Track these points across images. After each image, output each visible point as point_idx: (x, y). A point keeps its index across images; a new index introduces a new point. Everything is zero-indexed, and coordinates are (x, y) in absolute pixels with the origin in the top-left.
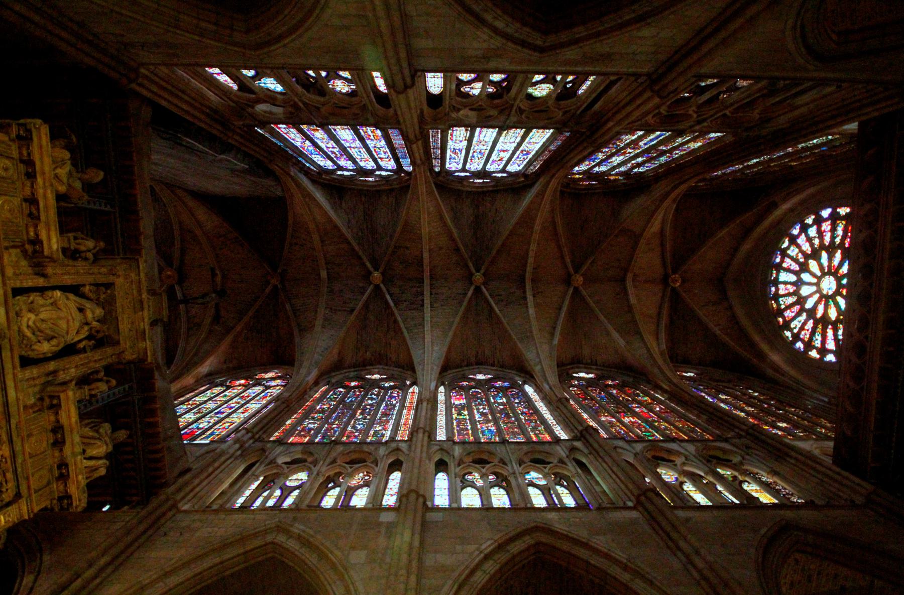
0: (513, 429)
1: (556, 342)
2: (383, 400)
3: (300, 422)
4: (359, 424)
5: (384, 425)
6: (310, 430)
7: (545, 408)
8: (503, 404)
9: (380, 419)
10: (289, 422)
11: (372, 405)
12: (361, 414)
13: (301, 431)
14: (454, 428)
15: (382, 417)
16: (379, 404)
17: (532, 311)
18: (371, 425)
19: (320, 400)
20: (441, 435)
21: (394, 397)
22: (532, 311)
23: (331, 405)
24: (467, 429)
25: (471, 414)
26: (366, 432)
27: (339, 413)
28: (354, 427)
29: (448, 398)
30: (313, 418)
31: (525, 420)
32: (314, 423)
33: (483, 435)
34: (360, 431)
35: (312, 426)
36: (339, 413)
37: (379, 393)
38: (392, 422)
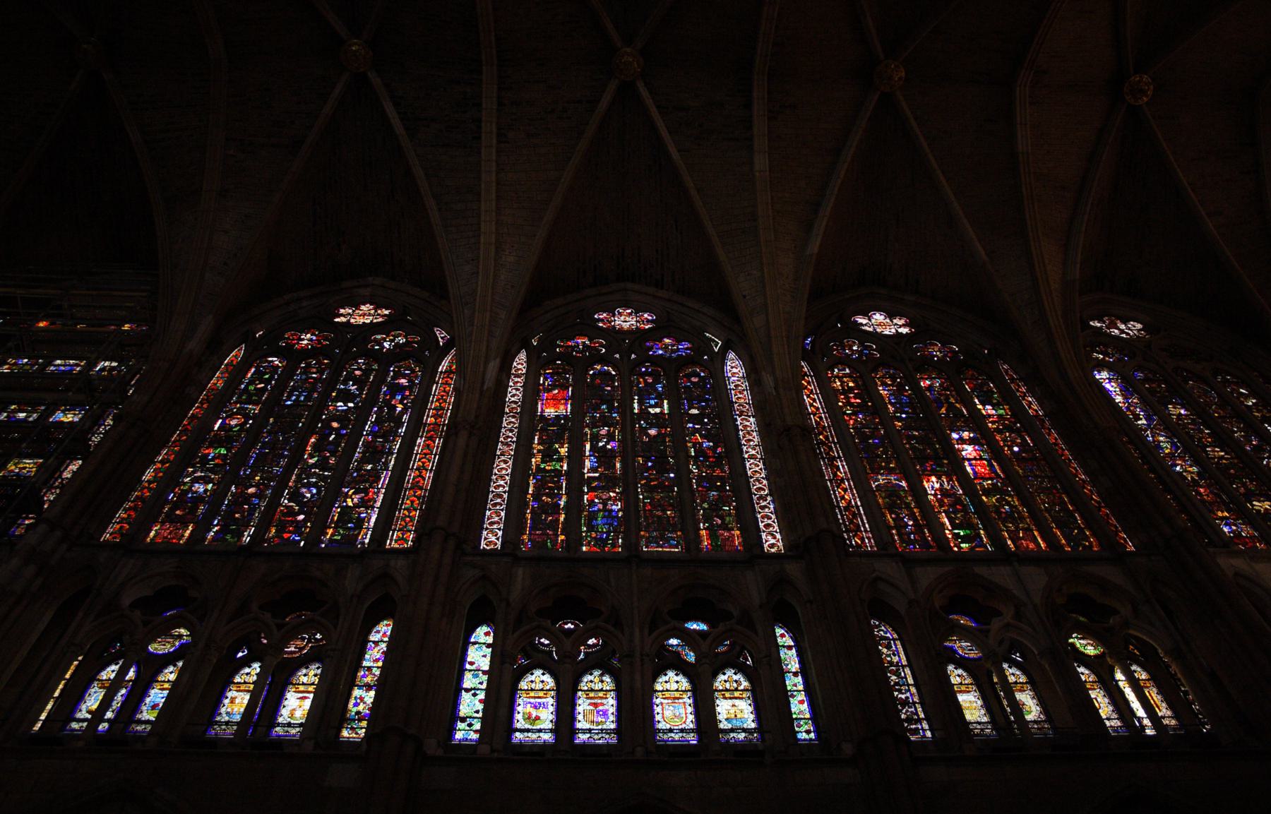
0: (664, 511)
1: (814, 247)
2: (372, 400)
3: (171, 478)
4: (309, 486)
5: (366, 491)
6: (199, 499)
7: (756, 440)
8: (658, 420)
9: (358, 469)
10: (148, 475)
11: (343, 417)
12: (317, 448)
13: (175, 506)
14: (526, 505)
15: (363, 461)
16: (361, 414)
17: (761, 162)
18: (333, 493)
19: (219, 403)
20: (491, 538)
21: (401, 389)
22: (761, 162)
23: (247, 417)
24: (555, 508)
25: (576, 458)
26: (318, 512)
27: (265, 445)
28: (296, 496)
29: (532, 393)
30: (205, 460)
31: (700, 477)
32: (206, 480)
33: (591, 528)
34: (305, 506)
35: (200, 488)
36: (265, 445)
37: (366, 373)
38: (385, 478)
